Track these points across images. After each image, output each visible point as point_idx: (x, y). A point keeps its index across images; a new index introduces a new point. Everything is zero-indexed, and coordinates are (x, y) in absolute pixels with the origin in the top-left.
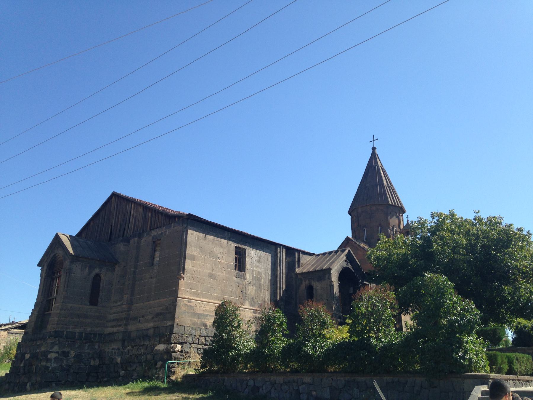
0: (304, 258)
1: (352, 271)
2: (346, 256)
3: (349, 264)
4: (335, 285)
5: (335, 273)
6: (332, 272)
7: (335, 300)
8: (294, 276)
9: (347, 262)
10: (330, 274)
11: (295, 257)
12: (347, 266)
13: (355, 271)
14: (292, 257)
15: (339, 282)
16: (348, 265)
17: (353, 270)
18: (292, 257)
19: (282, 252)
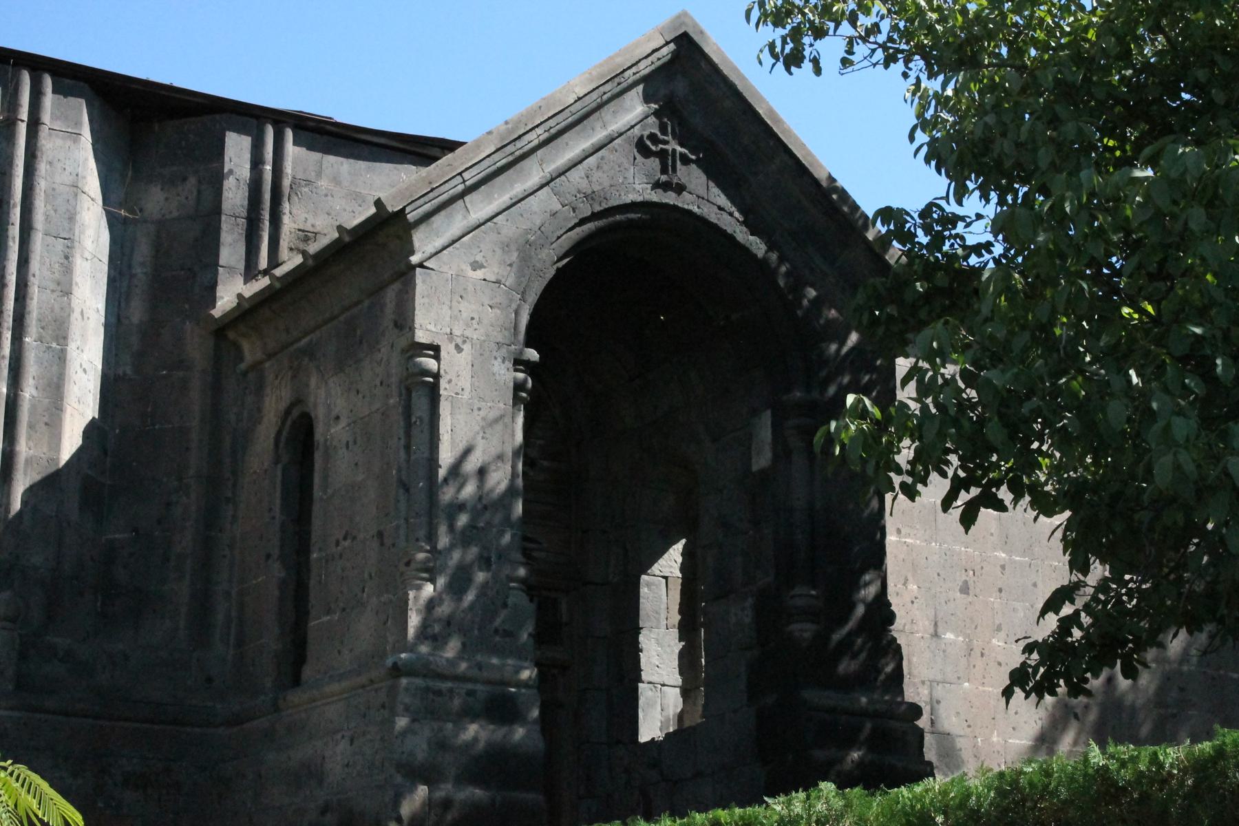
0: (336, 180)
1: (744, 250)
2: (647, 99)
3: (693, 177)
4: (465, 382)
5: (476, 266)
6: (424, 243)
7: (443, 541)
8: (197, 348)
9: (662, 155)
10: (406, 274)
11: (217, 179)
12: (670, 198)
13: (770, 248)
14: (192, 180)
15: (533, 355)
16: (680, 189)
17: (742, 235)
18: (192, 180)
19: (34, 124)
